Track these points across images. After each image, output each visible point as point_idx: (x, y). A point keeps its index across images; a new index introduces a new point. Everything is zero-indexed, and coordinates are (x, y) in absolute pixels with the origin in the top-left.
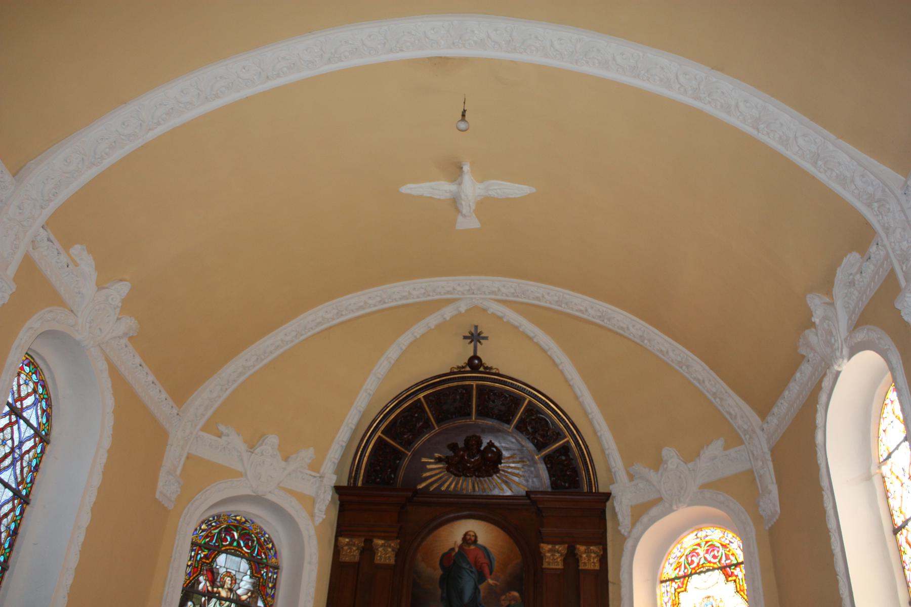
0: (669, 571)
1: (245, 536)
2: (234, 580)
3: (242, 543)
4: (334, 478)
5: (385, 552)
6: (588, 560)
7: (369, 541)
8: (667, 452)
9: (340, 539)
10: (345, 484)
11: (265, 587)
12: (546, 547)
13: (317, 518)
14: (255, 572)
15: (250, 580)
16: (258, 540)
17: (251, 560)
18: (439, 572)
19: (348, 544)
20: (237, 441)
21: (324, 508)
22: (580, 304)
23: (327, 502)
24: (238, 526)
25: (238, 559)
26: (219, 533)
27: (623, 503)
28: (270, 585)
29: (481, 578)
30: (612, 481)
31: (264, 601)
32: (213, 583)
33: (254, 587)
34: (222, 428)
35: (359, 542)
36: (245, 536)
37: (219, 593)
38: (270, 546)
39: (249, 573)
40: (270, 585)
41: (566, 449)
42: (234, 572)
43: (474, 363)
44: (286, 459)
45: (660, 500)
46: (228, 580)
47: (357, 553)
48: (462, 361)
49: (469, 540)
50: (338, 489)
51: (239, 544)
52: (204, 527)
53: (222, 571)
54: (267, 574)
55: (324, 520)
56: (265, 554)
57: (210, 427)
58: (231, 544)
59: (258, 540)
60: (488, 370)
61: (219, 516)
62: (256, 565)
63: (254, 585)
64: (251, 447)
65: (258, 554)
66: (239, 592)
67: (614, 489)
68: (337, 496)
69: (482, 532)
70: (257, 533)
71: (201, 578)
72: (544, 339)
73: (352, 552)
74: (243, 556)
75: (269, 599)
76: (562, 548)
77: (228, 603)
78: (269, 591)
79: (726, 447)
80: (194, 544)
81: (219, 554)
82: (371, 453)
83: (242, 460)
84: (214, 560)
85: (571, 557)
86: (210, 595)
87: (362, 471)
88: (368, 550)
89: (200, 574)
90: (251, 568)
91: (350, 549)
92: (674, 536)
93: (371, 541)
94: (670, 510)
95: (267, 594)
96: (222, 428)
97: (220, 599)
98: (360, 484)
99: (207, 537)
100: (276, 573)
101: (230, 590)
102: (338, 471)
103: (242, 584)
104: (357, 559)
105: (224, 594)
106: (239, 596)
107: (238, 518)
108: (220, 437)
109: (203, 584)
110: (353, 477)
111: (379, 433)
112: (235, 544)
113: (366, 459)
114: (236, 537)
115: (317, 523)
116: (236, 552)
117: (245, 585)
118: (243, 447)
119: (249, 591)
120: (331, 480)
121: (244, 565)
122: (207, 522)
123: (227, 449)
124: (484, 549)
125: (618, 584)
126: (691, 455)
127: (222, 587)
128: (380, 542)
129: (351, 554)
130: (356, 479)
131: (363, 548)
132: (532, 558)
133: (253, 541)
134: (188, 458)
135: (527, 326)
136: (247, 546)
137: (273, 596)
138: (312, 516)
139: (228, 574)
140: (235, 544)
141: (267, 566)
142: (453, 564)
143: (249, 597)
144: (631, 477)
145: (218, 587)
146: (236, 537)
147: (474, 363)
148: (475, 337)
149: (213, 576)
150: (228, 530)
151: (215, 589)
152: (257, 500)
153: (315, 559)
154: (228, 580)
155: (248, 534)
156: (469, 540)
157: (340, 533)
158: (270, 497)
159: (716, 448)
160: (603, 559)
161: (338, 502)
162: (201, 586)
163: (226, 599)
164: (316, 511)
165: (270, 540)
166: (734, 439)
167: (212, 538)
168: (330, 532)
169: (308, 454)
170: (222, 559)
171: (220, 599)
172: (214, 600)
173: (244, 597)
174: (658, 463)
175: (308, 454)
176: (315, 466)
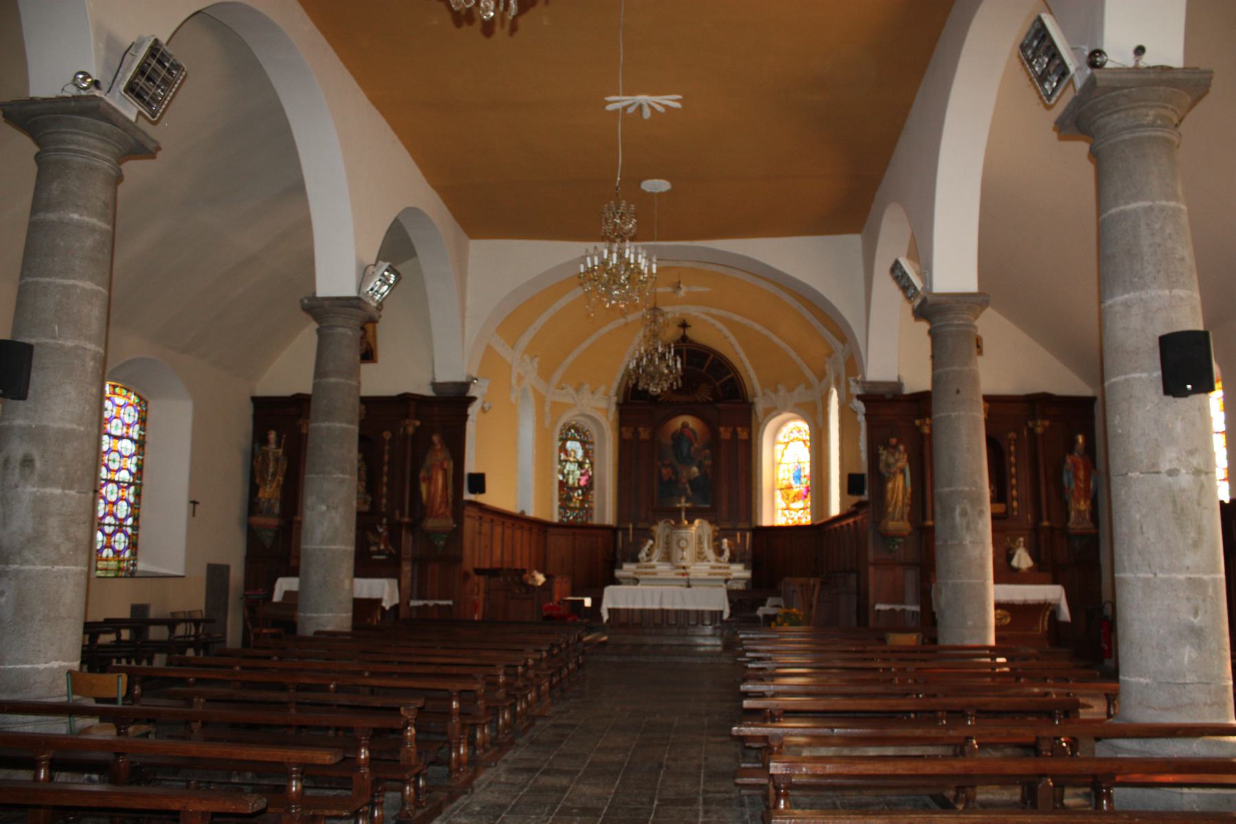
0: (781, 437)
1: (577, 431)
5: (644, 434)
6: (743, 435)
8: (779, 386)
9: (624, 429)
12: (722, 429)
14: (583, 448)
18: (670, 442)
20: (570, 390)
22: (737, 318)
24: (573, 427)
27: (760, 405)
29: (691, 444)
30: (755, 395)
41: (731, 380)
43: (684, 338)
45: (775, 408)
48: (678, 337)
49: (685, 426)
50: (618, 404)
60: (691, 342)
62: (583, 443)
67: (756, 400)
69: (691, 421)
72: (719, 325)
73: (628, 435)
76: (730, 429)
79: (807, 388)
85: (735, 433)
86: (566, 461)
88: (636, 433)
92: (784, 423)
94: (779, 414)
102: (617, 394)
109: (563, 456)
116: (574, 439)
118: (574, 393)
120: (614, 399)
124: (692, 430)
125: (756, 445)
126: (791, 390)
129: (628, 435)
132: (714, 434)
135: (711, 320)
142: (678, 437)
144: (764, 394)
147: (684, 338)
148: (684, 325)
150: (569, 430)
156: (685, 426)
159: (801, 388)
160: (750, 434)
166: (809, 386)
168: (616, 425)
169: (603, 389)
174: (776, 391)
176: (606, 394)
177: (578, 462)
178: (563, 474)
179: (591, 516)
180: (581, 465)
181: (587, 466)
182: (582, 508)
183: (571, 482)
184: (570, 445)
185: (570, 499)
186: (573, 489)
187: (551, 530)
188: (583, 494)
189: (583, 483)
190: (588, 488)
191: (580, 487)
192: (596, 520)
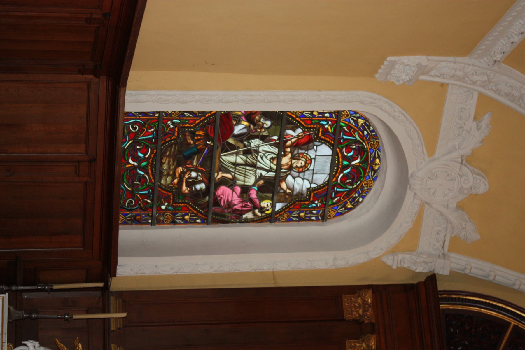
1: (357, 174)
2: (303, 169)
3: (348, 170)
4: (446, 272)
7: (372, 329)
9: (370, 292)
10: (441, 286)
11: (300, 208)
13: (391, 257)
15: (304, 189)
16: (354, 190)
17: (328, 186)
19: (365, 302)
21: (406, 265)
23: (413, 268)
25: (328, 172)
26: (356, 142)
28: (302, 214)
31: (282, 210)
32: (296, 145)
33: (297, 195)
34: (486, 119)
35: (369, 316)
36: (357, 174)
37: (285, 155)
38: (349, 206)
39: (313, 186)
40: (302, 214)
42: (311, 168)
44: (460, 207)
46: (301, 163)
47: (355, 315)
51: (346, 167)
52: (361, 121)
53: (311, 154)
54: (314, 208)
55: (390, 267)
56: (339, 201)
57: (485, 103)
58: (345, 158)
59: (354, 190)
61: (376, 137)
63: (300, 194)
64: (468, 160)
65: (337, 193)
66: (289, 179)
68: (422, 279)
70: (362, 187)
71: (299, 131)
73: (355, 309)
74: (332, 174)
75: (285, 216)
77: (274, 167)
78: (295, 214)
80: (338, 114)
81: (331, 146)
82: (486, 315)
83: (450, 152)
84: (324, 141)
86: (281, 145)
87: (460, 308)
89: (304, 128)
90: (319, 187)
91: (359, 307)
93: (373, 332)
95: (291, 213)
96: (486, 119)
97: (279, 157)
98: (443, 306)
99: (349, 127)
100: (317, 218)
101: (290, 168)
102: (454, 275)
103: (299, 180)
104: (347, 316)
105: (285, 160)
106: (284, 179)
107: (377, 161)
108: (475, 119)
110: (451, 296)
111: (513, 323)
112: (346, 163)
113: (477, 309)
114: (354, 163)
115: (385, 259)
116: (336, 166)
117: (299, 184)
118: (466, 151)
119: (292, 190)
120: (442, 269)
121: (321, 179)
122: (367, 124)
123: (462, 130)
127: (293, 158)
128: (373, 344)
130: (448, 300)
131: (363, 322)
133: (351, 184)
134: (442, 85)
136: (345, 177)
137: (289, 220)
138: (394, 251)
139: (309, 161)
140: (346, 163)
141: (324, 206)
143: (285, 192)
145: (291, 152)
146: (354, 163)
149: (305, 143)
150: (360, 151)
151: (288, 150)
152: (403, 180)
153: (341, 263)
154: (301, 163)
155: (359, 177)
157: (377, 290)
158: (409, 195)
161: (415, 282)
162: (290, 132)
163: (279, 165)
164: (400, 256)
165: (356, 204)
167: (349, 134)
170: (325, 150)
171: (279, 157)
172: (276, 150)
173: (284, 185)
175: (471, 232)
177: (279, 178)
178: (248, 136)
179: (137, 221)
180: (270, 187)
181: (265, 204)
182: (159, 194)
183: (229, 158)
184: (323, 151)
185: (183, 159)
186: (209, 165)
187: (102, 84)
188: (197, 195)
189: (224, 192)
190: (209, 210)
191: (213, 185)
192: (127, 234)
